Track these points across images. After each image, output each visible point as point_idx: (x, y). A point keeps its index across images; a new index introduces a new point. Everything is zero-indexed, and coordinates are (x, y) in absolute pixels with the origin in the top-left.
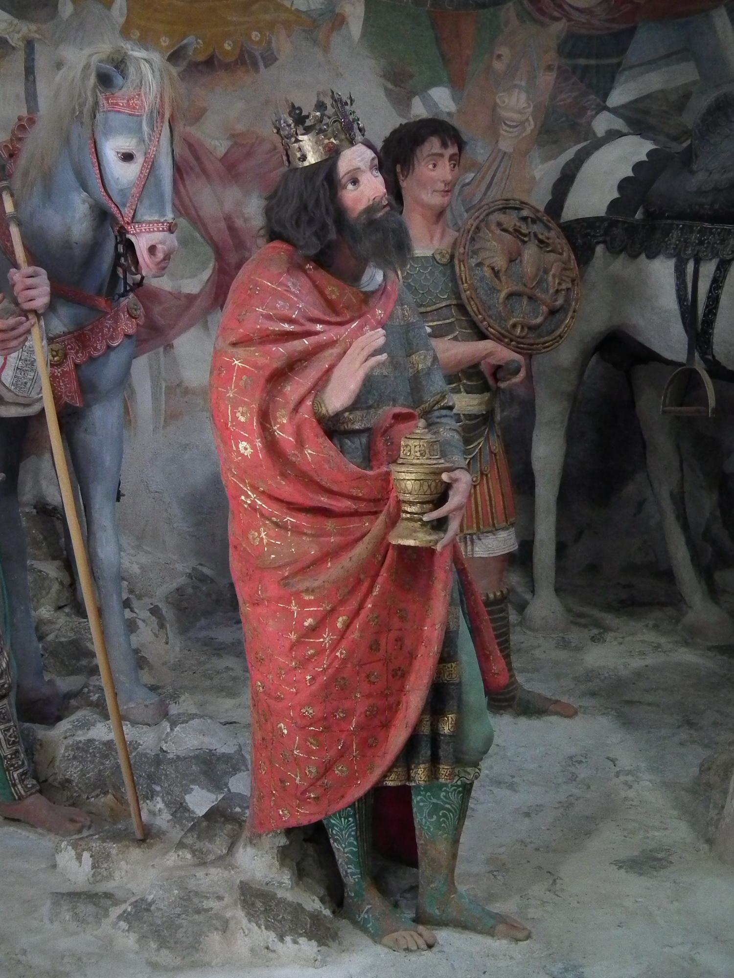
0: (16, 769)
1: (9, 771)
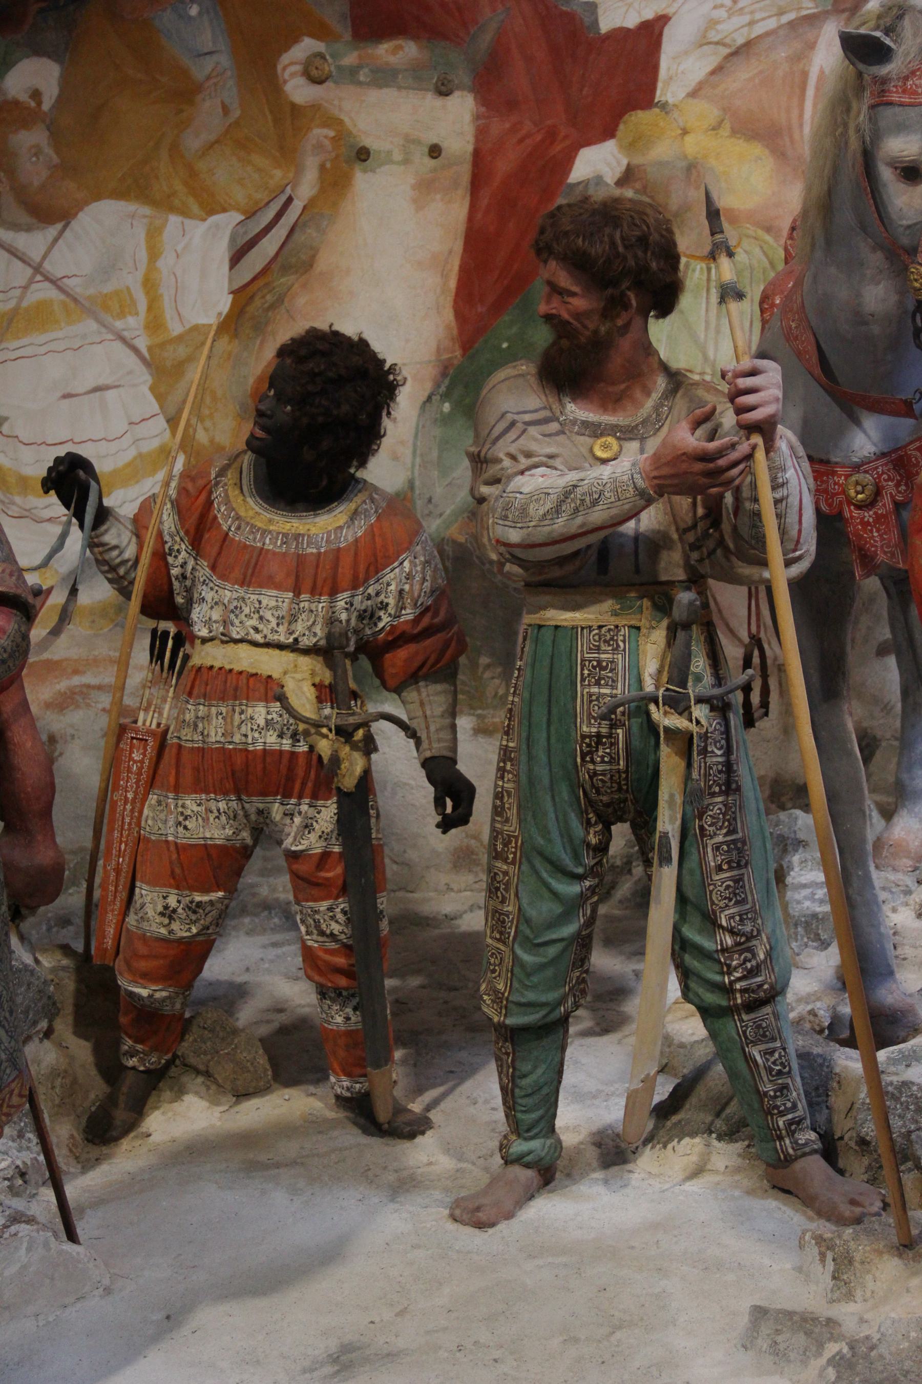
0: (782, 1114)
1: (772, 1115)
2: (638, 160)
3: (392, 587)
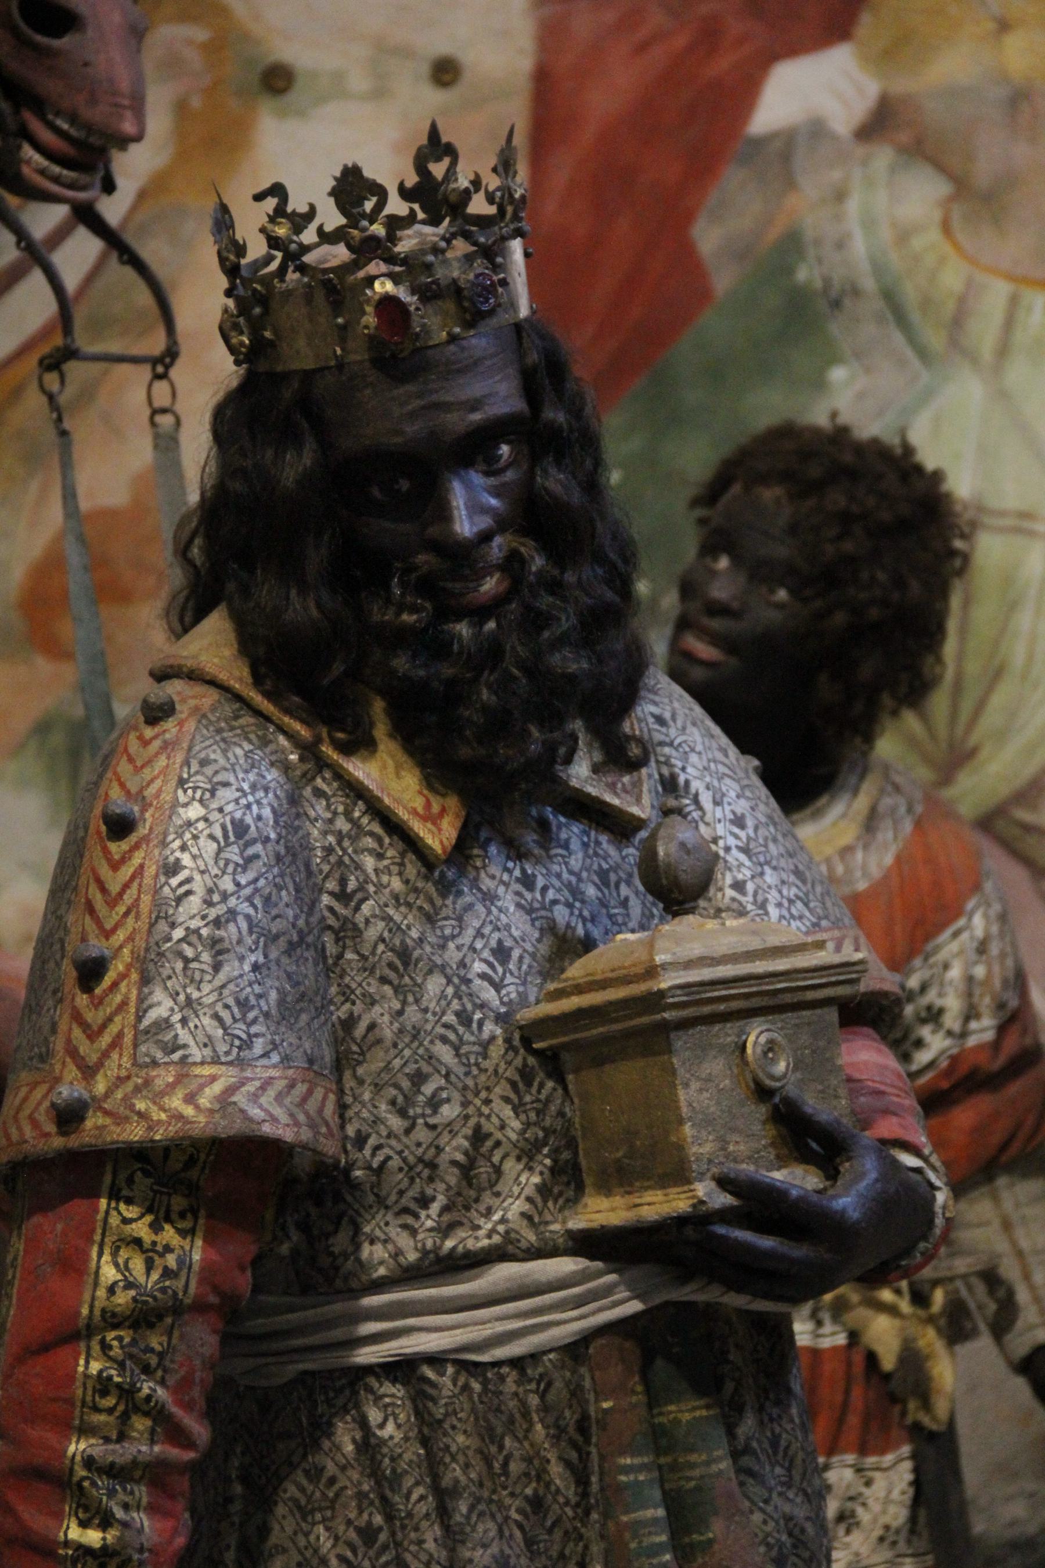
2: (902, 85)
3: (955, 973)
